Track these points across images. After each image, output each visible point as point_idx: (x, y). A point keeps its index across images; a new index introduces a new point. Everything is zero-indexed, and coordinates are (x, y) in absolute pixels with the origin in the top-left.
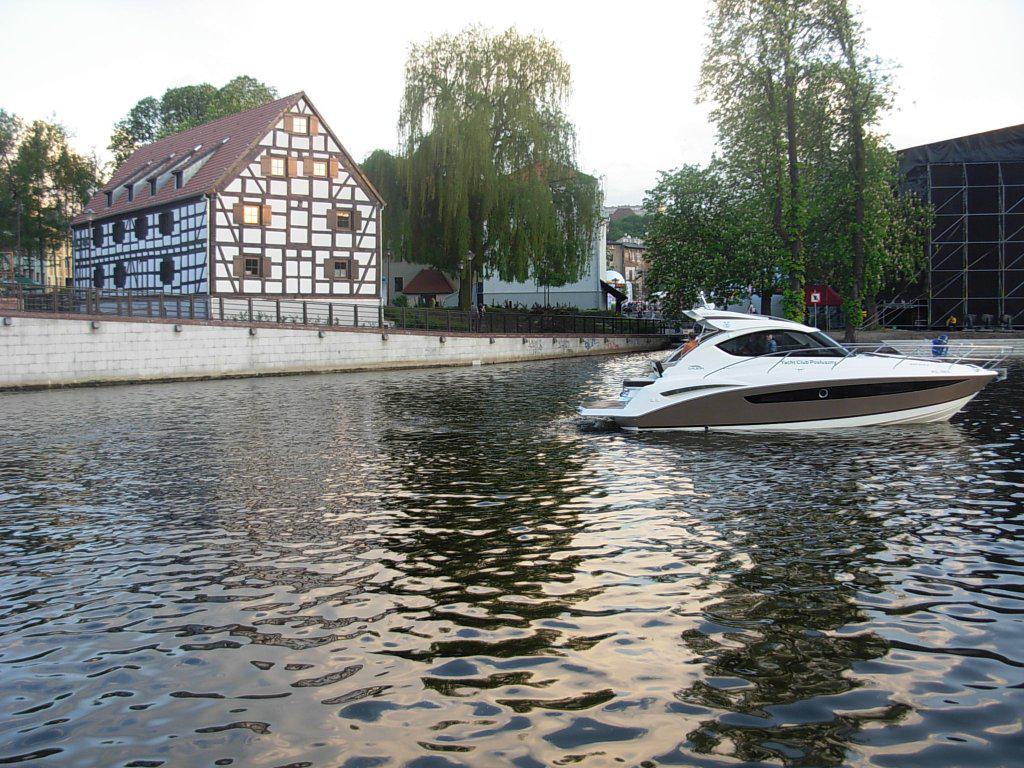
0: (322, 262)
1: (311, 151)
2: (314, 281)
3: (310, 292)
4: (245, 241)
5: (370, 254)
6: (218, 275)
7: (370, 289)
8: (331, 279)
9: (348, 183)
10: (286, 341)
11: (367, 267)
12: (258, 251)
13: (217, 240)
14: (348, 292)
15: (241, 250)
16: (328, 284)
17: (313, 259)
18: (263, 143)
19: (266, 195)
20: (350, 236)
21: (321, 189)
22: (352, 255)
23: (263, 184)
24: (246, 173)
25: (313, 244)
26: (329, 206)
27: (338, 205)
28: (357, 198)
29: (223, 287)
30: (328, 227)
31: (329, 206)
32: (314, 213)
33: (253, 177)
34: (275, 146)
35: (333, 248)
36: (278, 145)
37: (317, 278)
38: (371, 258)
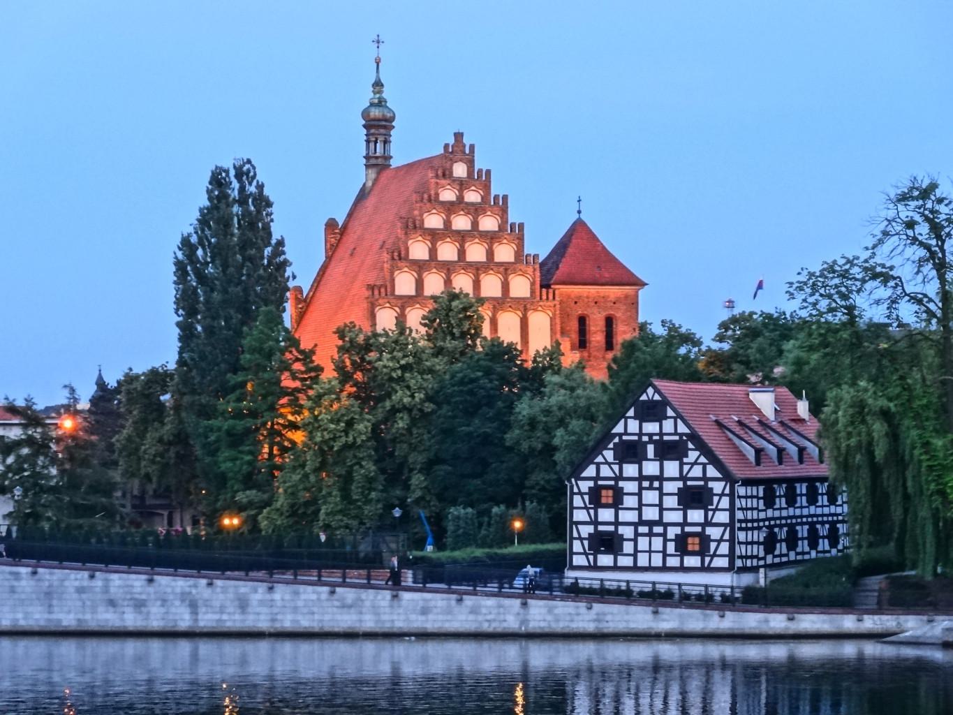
0: (673, 537)
1: (661, 434)
2: (665, 555)
3: (660, 564)
4: (600, 520)
6: (575, 550)
7: (722, 562)
8: (682, 549)
9: (699, 461)
10: (556, 611)
11: (719, 541)
12: (612, 528)
13: (574, 520)
14: (699, 564)
15: (596, 528)
16: (679, 558)
17: (664, 535)
18: (614, 431)
20: (702, 512)
21: (671, 468)
22: (704, 530)
23: (616, 468)
24: (599, 459)
25: (665, 521)
26: (680, 484)
27: (689, 483)
28: (709, 475)
29: (579, 560)
30: (679, 505)
31: (680, 484)
32: (665, 491)
33: (607, 463)
34: (626, 433)
35: (685, 523)
36: (629, 431)
37: (668, 552)
38: (725, 531)
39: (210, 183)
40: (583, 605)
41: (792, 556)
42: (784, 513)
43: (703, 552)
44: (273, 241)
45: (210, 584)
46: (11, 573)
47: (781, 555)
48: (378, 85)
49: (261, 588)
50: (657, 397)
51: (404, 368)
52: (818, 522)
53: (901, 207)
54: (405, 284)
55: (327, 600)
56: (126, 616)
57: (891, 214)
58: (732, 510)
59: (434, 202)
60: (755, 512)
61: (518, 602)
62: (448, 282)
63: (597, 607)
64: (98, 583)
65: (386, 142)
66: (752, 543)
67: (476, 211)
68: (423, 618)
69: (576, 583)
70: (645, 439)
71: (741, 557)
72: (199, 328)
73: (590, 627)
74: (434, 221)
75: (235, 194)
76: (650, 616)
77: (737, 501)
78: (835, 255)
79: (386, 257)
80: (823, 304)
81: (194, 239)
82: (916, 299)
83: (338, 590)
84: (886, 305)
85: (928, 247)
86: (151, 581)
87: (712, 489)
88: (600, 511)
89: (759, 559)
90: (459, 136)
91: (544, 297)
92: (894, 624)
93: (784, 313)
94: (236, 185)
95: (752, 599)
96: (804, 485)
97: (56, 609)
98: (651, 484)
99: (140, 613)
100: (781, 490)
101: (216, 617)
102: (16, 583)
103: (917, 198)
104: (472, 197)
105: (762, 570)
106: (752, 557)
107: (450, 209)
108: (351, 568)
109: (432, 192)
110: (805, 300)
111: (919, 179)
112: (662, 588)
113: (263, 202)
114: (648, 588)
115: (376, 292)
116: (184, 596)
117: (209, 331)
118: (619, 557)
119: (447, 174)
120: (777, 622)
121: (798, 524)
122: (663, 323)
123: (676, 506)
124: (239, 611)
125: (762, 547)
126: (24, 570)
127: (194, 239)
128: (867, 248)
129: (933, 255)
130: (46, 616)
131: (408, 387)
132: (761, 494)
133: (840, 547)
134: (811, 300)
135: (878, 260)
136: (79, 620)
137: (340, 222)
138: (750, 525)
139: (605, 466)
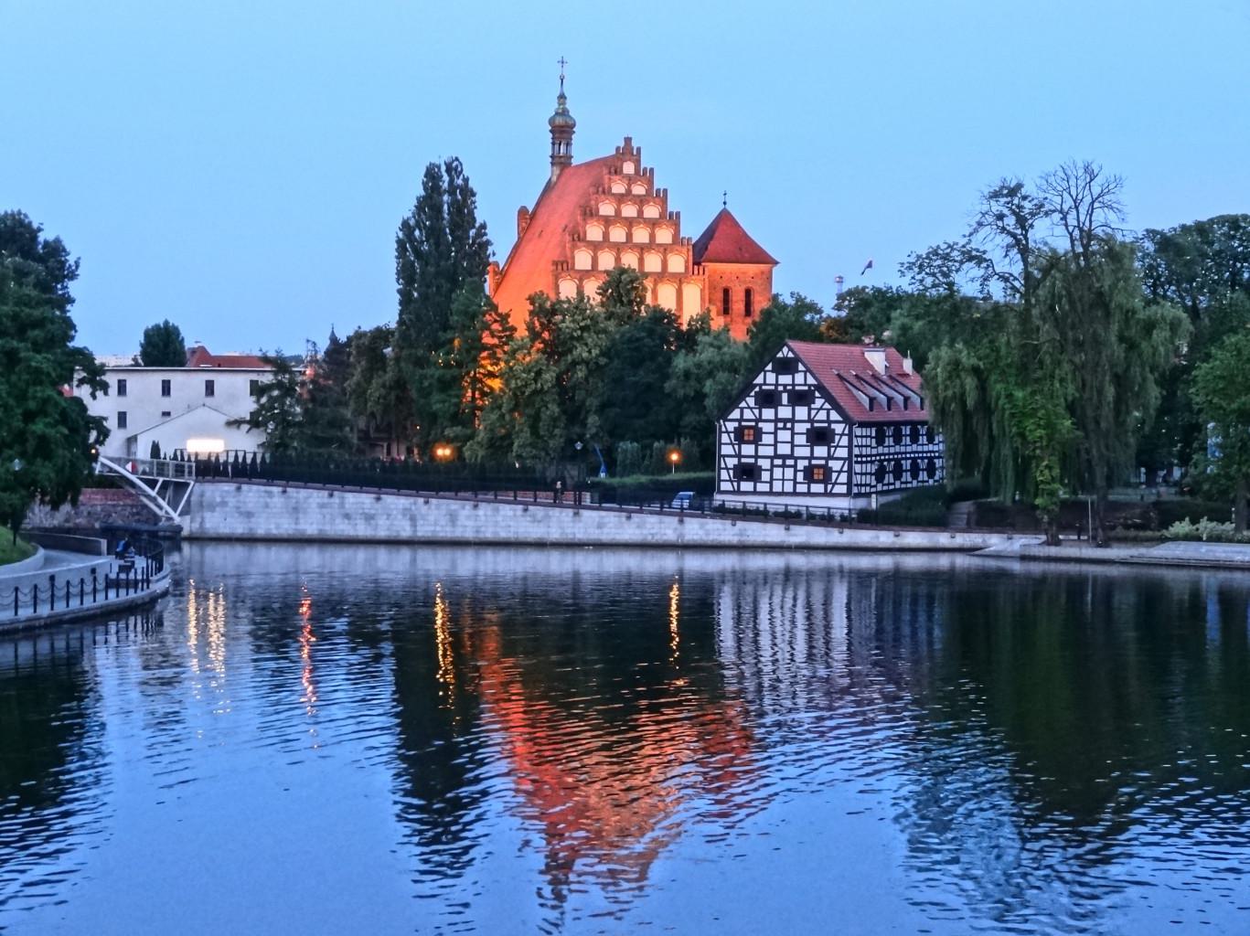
1: (793, 385)
2: (795, 483)
3: (791, 490)
5: (841, 462)
7: (843, 489)
11: (840, 472)
12: (752, 460)
14: (822, 491)
15: (739, 460)
17: (795, 466)
19: (759, 420)
20: (826, 448)
21: (802, 412)
22: (827, 463)
23: (756, 412)
24: (743, 404)
26: (808, 426)
27: (816, 425)
28: (832, 418)
29: (725, 486)
31: (808, 426)
33: (749, 407)
34: (765, 384)
35: (812, 457)
39: (426, 176)
40: (728, 522)
41: (898, 485)
42: (892, 450)
43: (826, 479)
44: (477, 225)
45: (427, 502)
46: (266, 492)
47: (889, 484)
48: (562, 97)
49: (469, 505)
50: (791, 355)
51: (583, 329)
52: (919, 458)
53: (993, 203)
54: (583, 260)
55: (522, 516)
56: (358, 527)
57: (985, 208)
58: (850, 447)
59: (607, 192)
60: (869, 449)
61: (676, 519)
62: (618, 259)
63: (740, 524)
64: (336, 500)
65: (568, 144)
66: (866, 474)
67: (641, 201)
68: (599, 531)
69: (723, 505)
70: (781, 388)
71: (857, 485)
72: (416, 294)
73: (735, 540)
74: (607, 209)
75: (446, 185)
76: (783, 532)
77: (854, 439)
78: (939, 240)
79: (568, 238)
80: (929, 281)
81: (412, 222)
82: (1004, 278)
83: (531, 508)
84: (979, 283)
85: (1014, 236)
86: (378, 499)
87: (834, 430)
88: (743, 446)
89: (872, 487)
90: (628, 140)
91: (696, 272)
92: (980, 540)
93: (891, 288)
94: (446, 178)
95: (866, 519)
96: (908, 427)
97: (301, 521)
98: (785, 425)
99: (370, 524)
100: (890, 431)
101: (432, 528)
102: (268, 500)
103: (1006, 196)
104: (639, 190)
105: (874, 496)
106: (866, 485)
107: (621, 199)
108: (540, 490)
109: (606, 186)
110: (913, 278)
111: (1008, 180)
112: (792, 509)
113: (468, 192)
114: (782, 509)
115: (560, 267)
116: (405, 511)
117: (424, 297)
118: (758, 484)
119: (618, 171)
120: (885, 538)
121: (903, 459)
122: (792, 294)
123: (805, 443)
124: (449, 524)
125: (873, 477)
126: (276, 490)
127: (412, 222)
128: (964, 236)
129: (1018, 242)
130: (293, 526)
131: (586, 345)
132: (874, 435)
133: (936, 478)
134: (919, 277)
135: (973, 245)
136: (321, 530)
137: (530, 210)
138: (864, 459)
139: (747, 410)
